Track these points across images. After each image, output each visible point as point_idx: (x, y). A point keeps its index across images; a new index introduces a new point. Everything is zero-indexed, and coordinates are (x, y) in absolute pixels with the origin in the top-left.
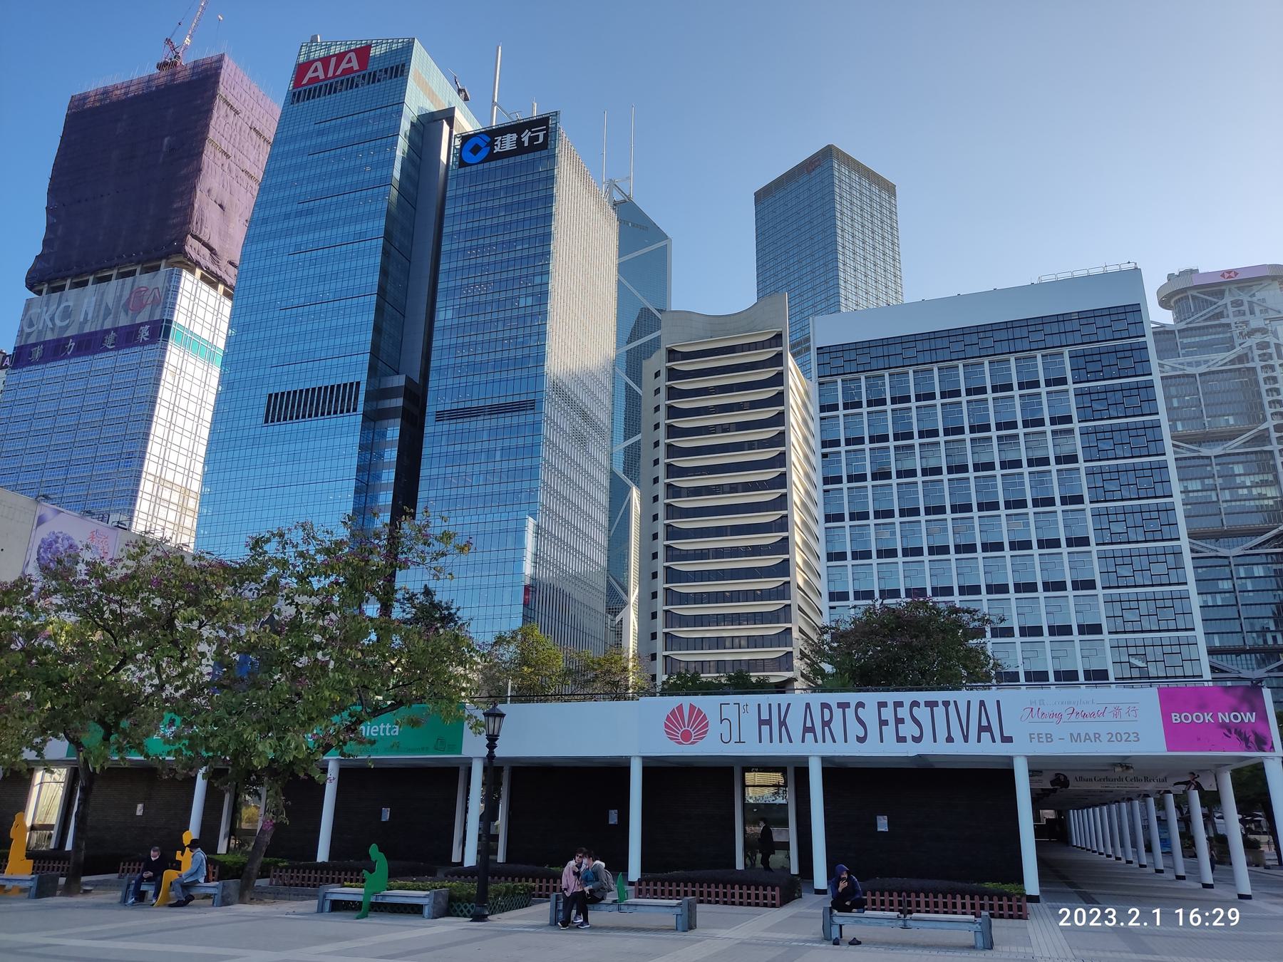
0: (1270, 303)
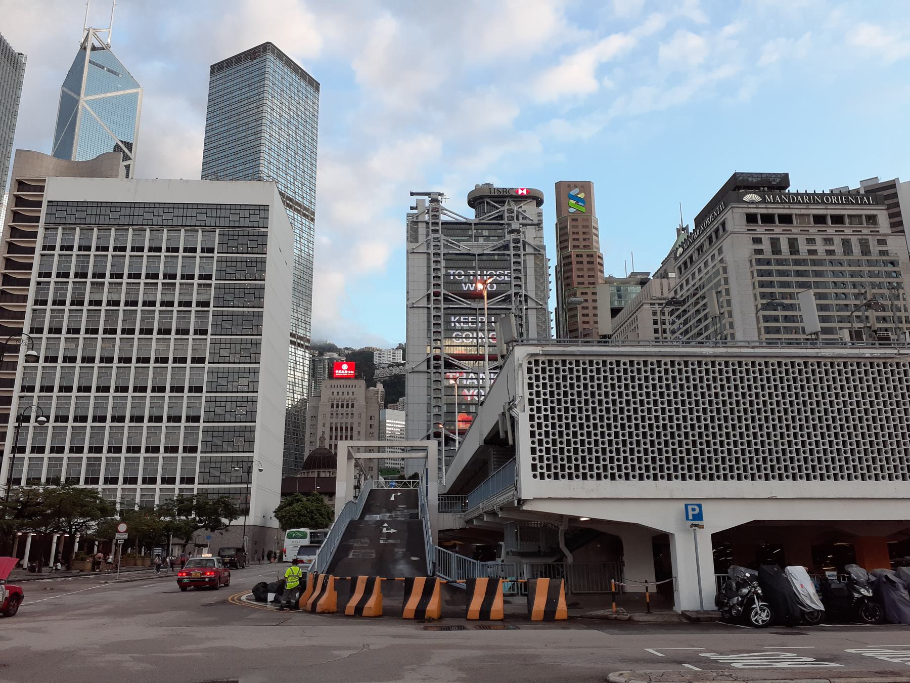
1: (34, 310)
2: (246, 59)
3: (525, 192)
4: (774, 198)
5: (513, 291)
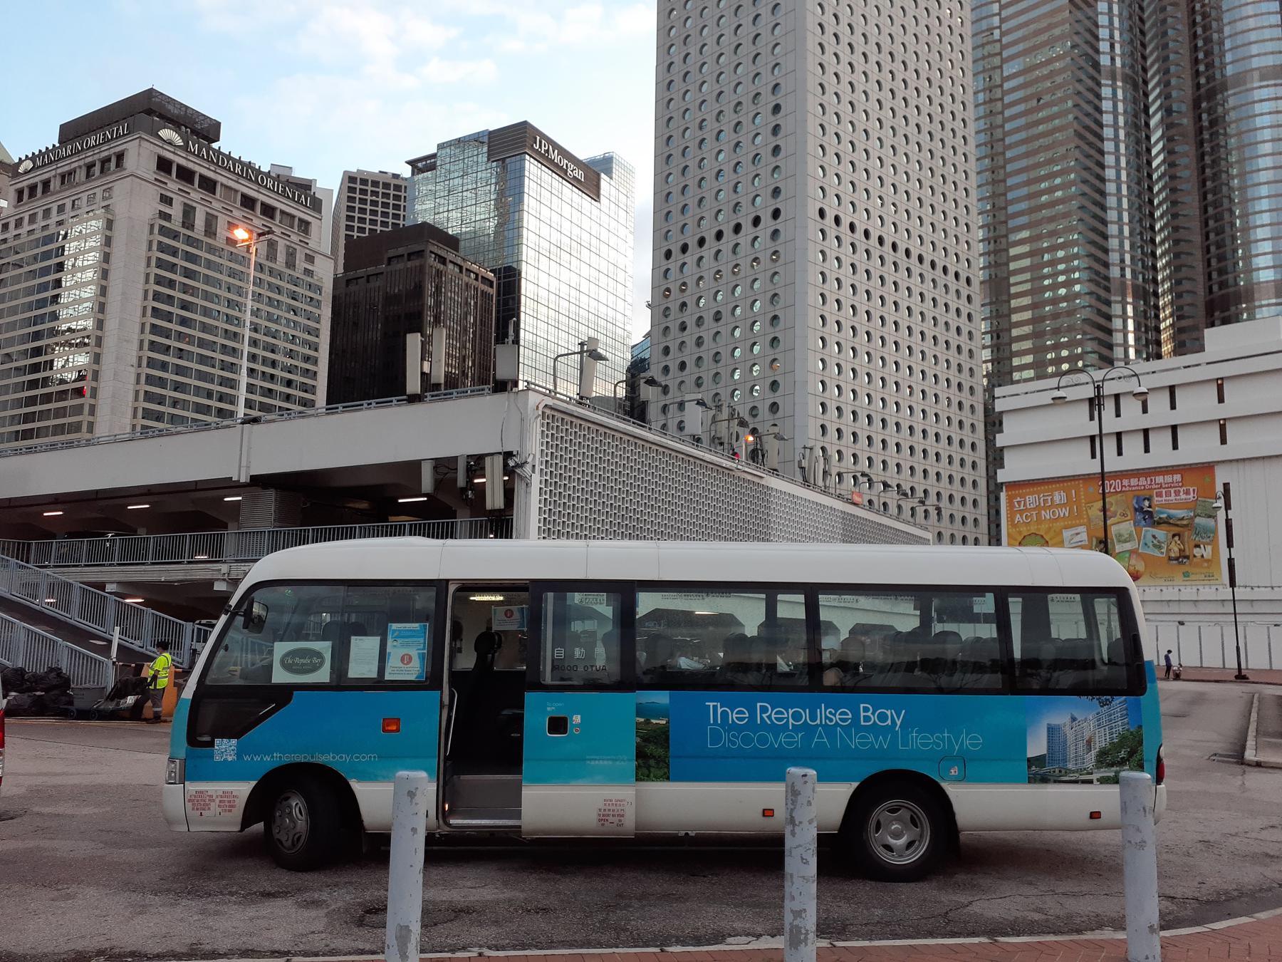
4: (200, 150)
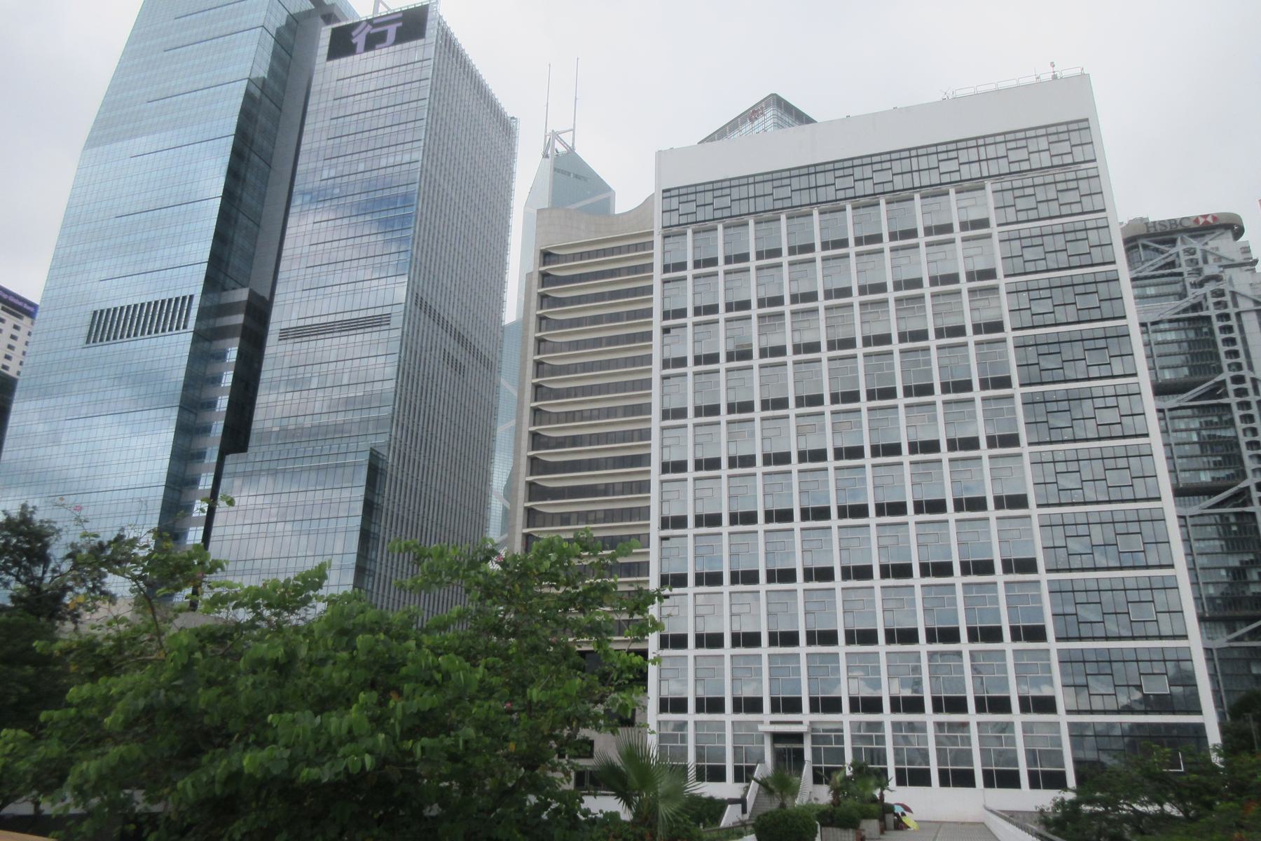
0: (1223, 252)
1: (665, 378)
2: (744, 122)
3: (1210, 219)
5: (1227, 375)
